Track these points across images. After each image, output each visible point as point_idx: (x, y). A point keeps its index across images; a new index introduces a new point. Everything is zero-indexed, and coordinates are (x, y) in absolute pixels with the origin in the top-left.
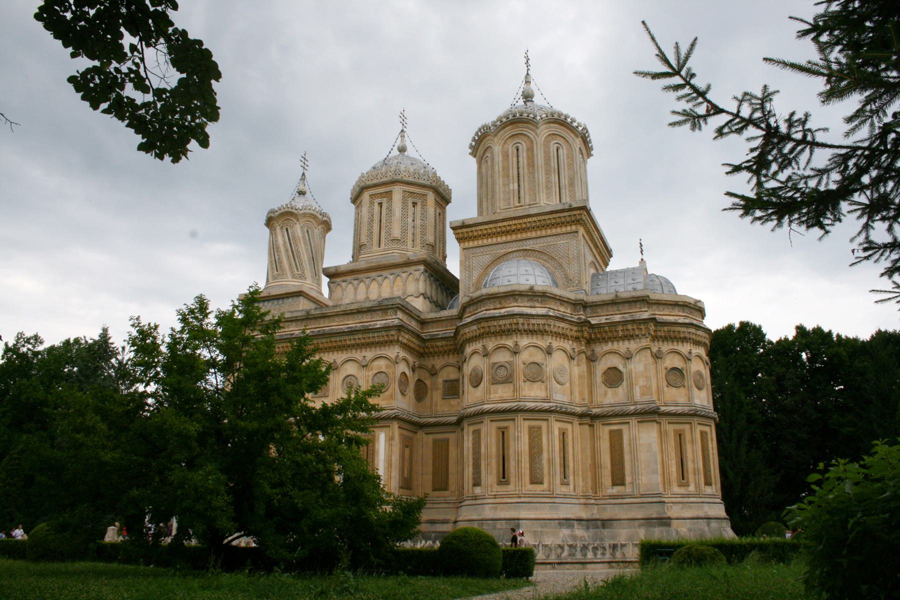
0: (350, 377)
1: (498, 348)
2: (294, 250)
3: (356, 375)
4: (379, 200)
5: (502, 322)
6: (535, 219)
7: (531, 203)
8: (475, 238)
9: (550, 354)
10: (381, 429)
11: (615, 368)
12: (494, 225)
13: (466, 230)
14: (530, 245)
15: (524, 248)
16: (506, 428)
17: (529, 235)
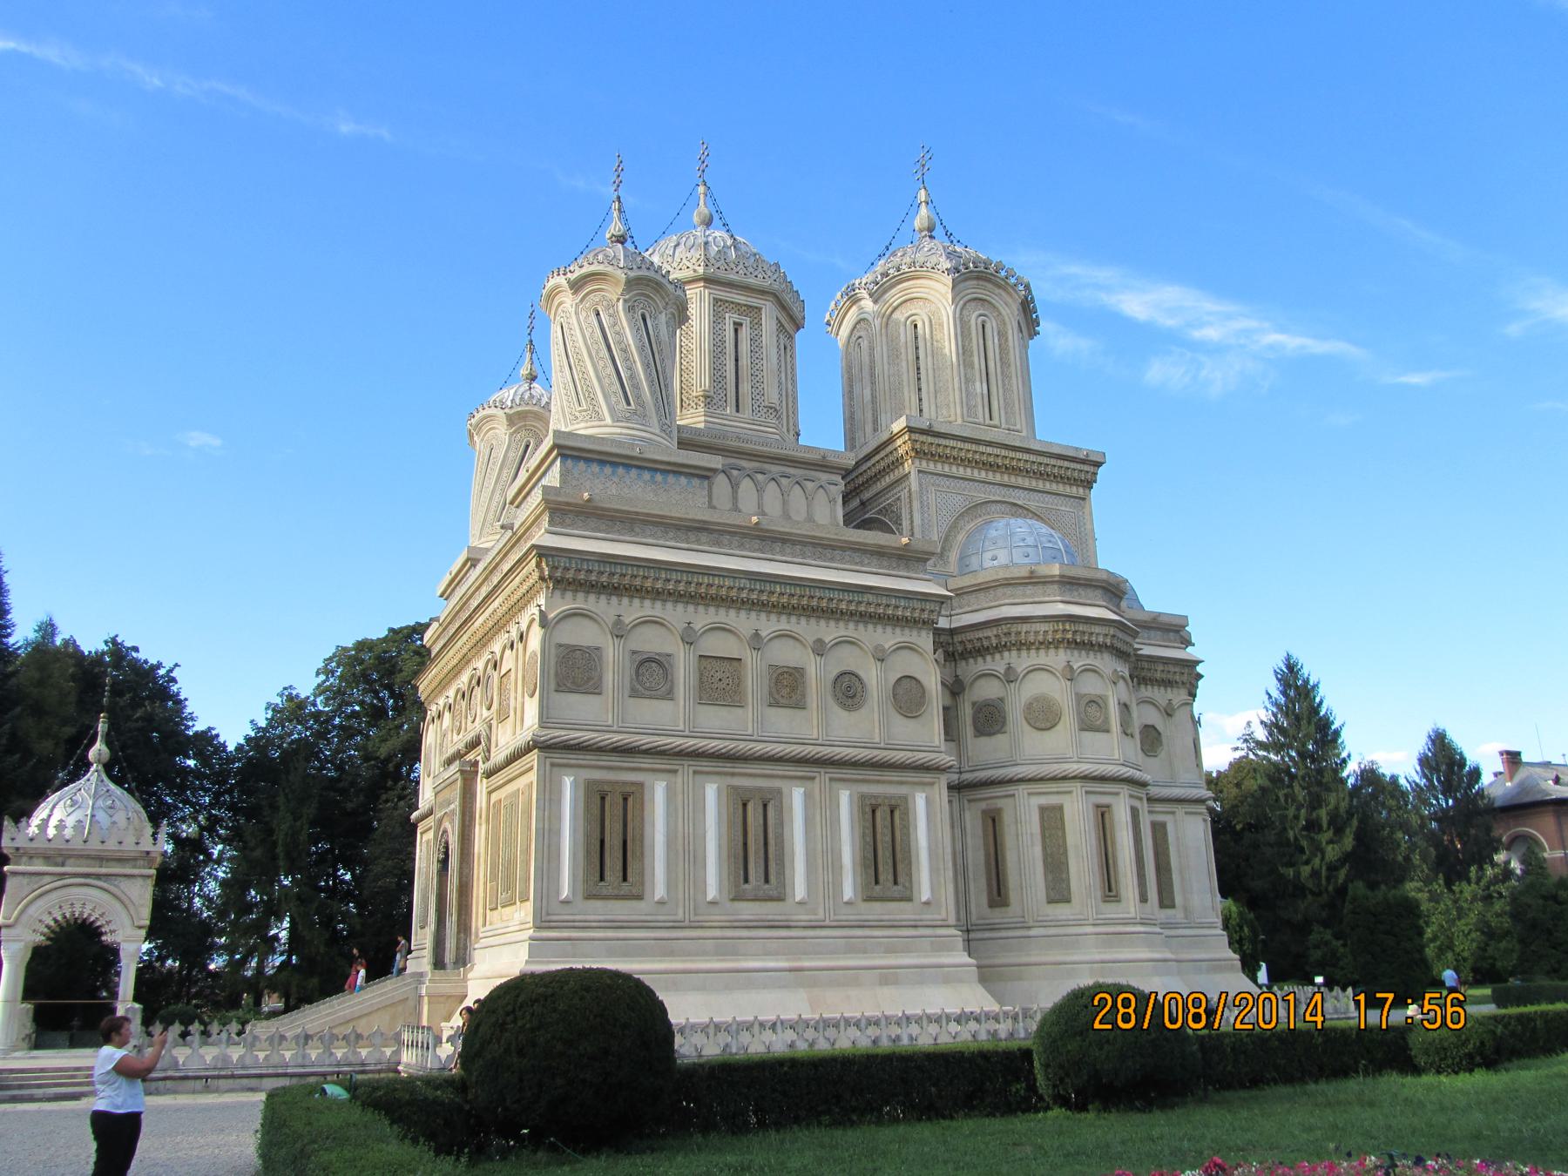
0: (847, 678)
2: (659, 368)
4: (736, 318)
5: (1097, 629)
6: (1032, 458)
7: (1012, 427)
8: (943, 458)
11: (1153, 727)
12: (974, 447)
13: (930, 439)
14: (1020, 498)
15: (1011, 500)
16: (1108, 806)
17: (1020, 481)
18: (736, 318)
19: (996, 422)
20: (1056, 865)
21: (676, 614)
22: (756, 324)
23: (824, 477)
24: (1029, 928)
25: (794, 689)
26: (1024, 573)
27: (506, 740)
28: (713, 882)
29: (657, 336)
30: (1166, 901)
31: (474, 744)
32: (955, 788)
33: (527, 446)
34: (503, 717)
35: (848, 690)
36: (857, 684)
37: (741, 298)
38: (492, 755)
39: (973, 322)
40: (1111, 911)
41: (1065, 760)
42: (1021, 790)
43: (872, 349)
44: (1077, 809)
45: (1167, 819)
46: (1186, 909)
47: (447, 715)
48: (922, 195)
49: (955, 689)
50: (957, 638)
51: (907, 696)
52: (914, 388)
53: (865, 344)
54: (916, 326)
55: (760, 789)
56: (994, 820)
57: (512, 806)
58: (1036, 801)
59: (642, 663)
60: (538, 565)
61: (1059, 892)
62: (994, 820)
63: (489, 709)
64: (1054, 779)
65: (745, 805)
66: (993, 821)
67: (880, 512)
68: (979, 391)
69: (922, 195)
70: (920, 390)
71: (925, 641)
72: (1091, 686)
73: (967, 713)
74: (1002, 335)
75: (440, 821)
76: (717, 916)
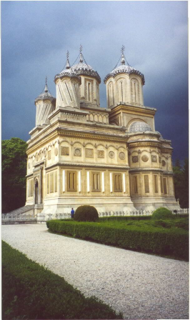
1: (75, 143)
3: (113, 151)
8: (127, 110)
9: (107, 148)
10: (111, 171)
14: (141, 118)
18: (89, 82)
19: (137, 102)
21: (82, 141)
22: (92, 83)
23: (105, 114)
24: (142, 197)
25: (102, 154)
26: (142, 133)
27: (49, 163)
28: (88, 189)
29: (77, 88)
30: (166, 193)
31: (43, 163)
32: (130, 172)
33: (47, 106)
34: (49, 158)
36: (113, 153)
37: (90, 78)
38: (47, 165)
39: (133, 83)
42: (141, 173)
43: (113, 87)
44: (151, 176)
45: (166, 178)
46: (168, 193)
47: (34, 158)
49: (129, 154)
50: (130, 144)
52: (121, 95)
53: (112, 86)
54: (122, 83)
56: (136, 178)
57: (52, 175)
58: (144, 175)
60: (58, 132)
61: (147, 191)
62: (136, 178)
63: (45, 157)
65: (94, 175)
66: (136, 177)
67: (114, 119)
70: (122, 96)
71: (125, 146)
72: (154, 154)
73: (131, 158)
74: (138, 85)
75: (35, 177)
76: (90, 194)
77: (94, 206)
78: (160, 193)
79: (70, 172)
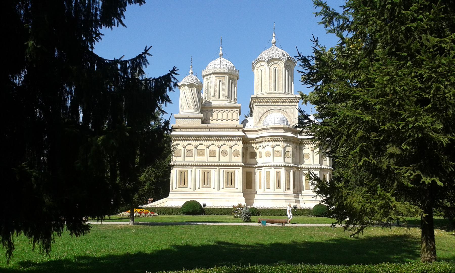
17: (280, 104)
19: (276, 91)
20: (268, 182)
21: (194, 143)
35: (224, 153)
40: (278, 190)
41: (271, 163)
42: (263, 168)
44: (282, 171)
48: (274, 35)
51: (236, 153)
55: (207, 170)
59: (188, 151)
64: (268, 166)
68: (273, 85)
69: (274, 35)
71: (240, 143)
72: (277, 148)
77: (197, 200)
78: (292, 189)
79: (182, 171)
